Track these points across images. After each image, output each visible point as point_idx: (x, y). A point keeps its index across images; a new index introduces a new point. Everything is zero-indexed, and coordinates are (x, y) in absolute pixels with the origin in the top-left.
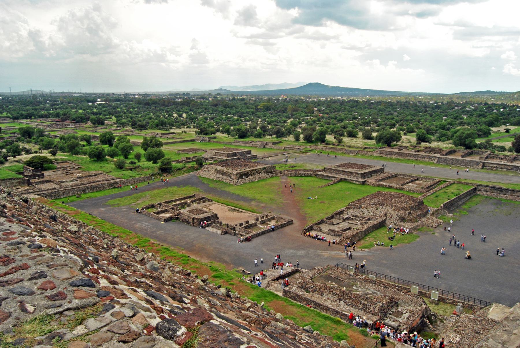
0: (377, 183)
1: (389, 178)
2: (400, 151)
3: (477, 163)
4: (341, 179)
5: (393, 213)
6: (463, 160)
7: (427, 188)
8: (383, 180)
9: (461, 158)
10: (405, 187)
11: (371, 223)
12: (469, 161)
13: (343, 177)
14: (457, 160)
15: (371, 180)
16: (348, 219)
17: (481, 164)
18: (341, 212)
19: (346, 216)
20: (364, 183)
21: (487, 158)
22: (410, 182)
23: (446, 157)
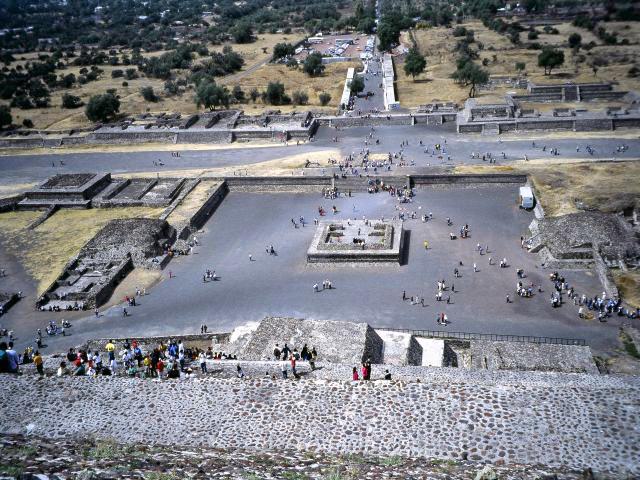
0: (107, 202)
1: (120, 189)
2: (128, 130)
3: (226, 134)
4: (56, 206)
5: (137, 251)
6: (208, 133)
7: (170, 197)
8: (113, 195)
9: (205, 130)
10: (144, 200)
11: (115, 269)
12: (215, 133)
13: (56, 202)
14: (200, 134)
15: (98, 199)
16: (86, 271)
17: (230, 136)
18: (75, 264)
19: (81, 268)
20: (89, 206)
21: (236, 125)
22: (148, 191)
23: (187, 131)
